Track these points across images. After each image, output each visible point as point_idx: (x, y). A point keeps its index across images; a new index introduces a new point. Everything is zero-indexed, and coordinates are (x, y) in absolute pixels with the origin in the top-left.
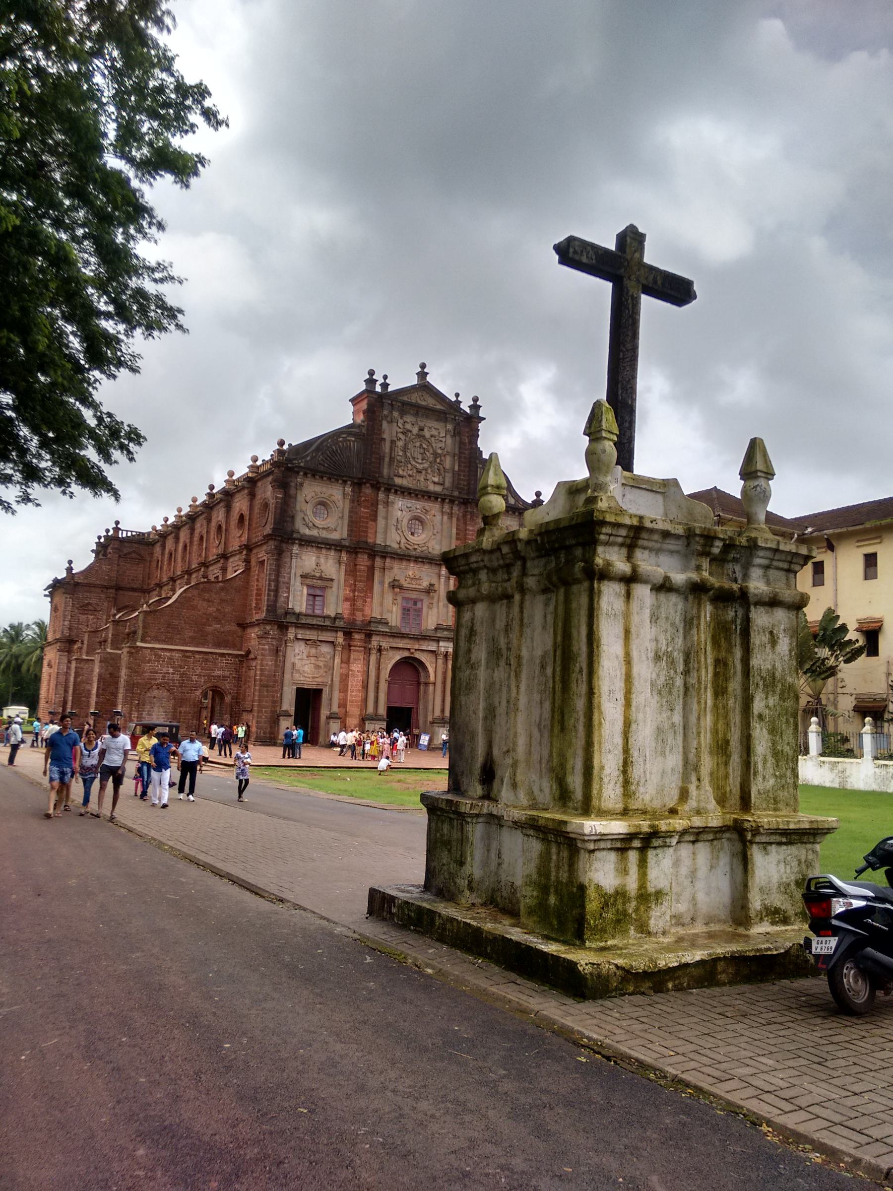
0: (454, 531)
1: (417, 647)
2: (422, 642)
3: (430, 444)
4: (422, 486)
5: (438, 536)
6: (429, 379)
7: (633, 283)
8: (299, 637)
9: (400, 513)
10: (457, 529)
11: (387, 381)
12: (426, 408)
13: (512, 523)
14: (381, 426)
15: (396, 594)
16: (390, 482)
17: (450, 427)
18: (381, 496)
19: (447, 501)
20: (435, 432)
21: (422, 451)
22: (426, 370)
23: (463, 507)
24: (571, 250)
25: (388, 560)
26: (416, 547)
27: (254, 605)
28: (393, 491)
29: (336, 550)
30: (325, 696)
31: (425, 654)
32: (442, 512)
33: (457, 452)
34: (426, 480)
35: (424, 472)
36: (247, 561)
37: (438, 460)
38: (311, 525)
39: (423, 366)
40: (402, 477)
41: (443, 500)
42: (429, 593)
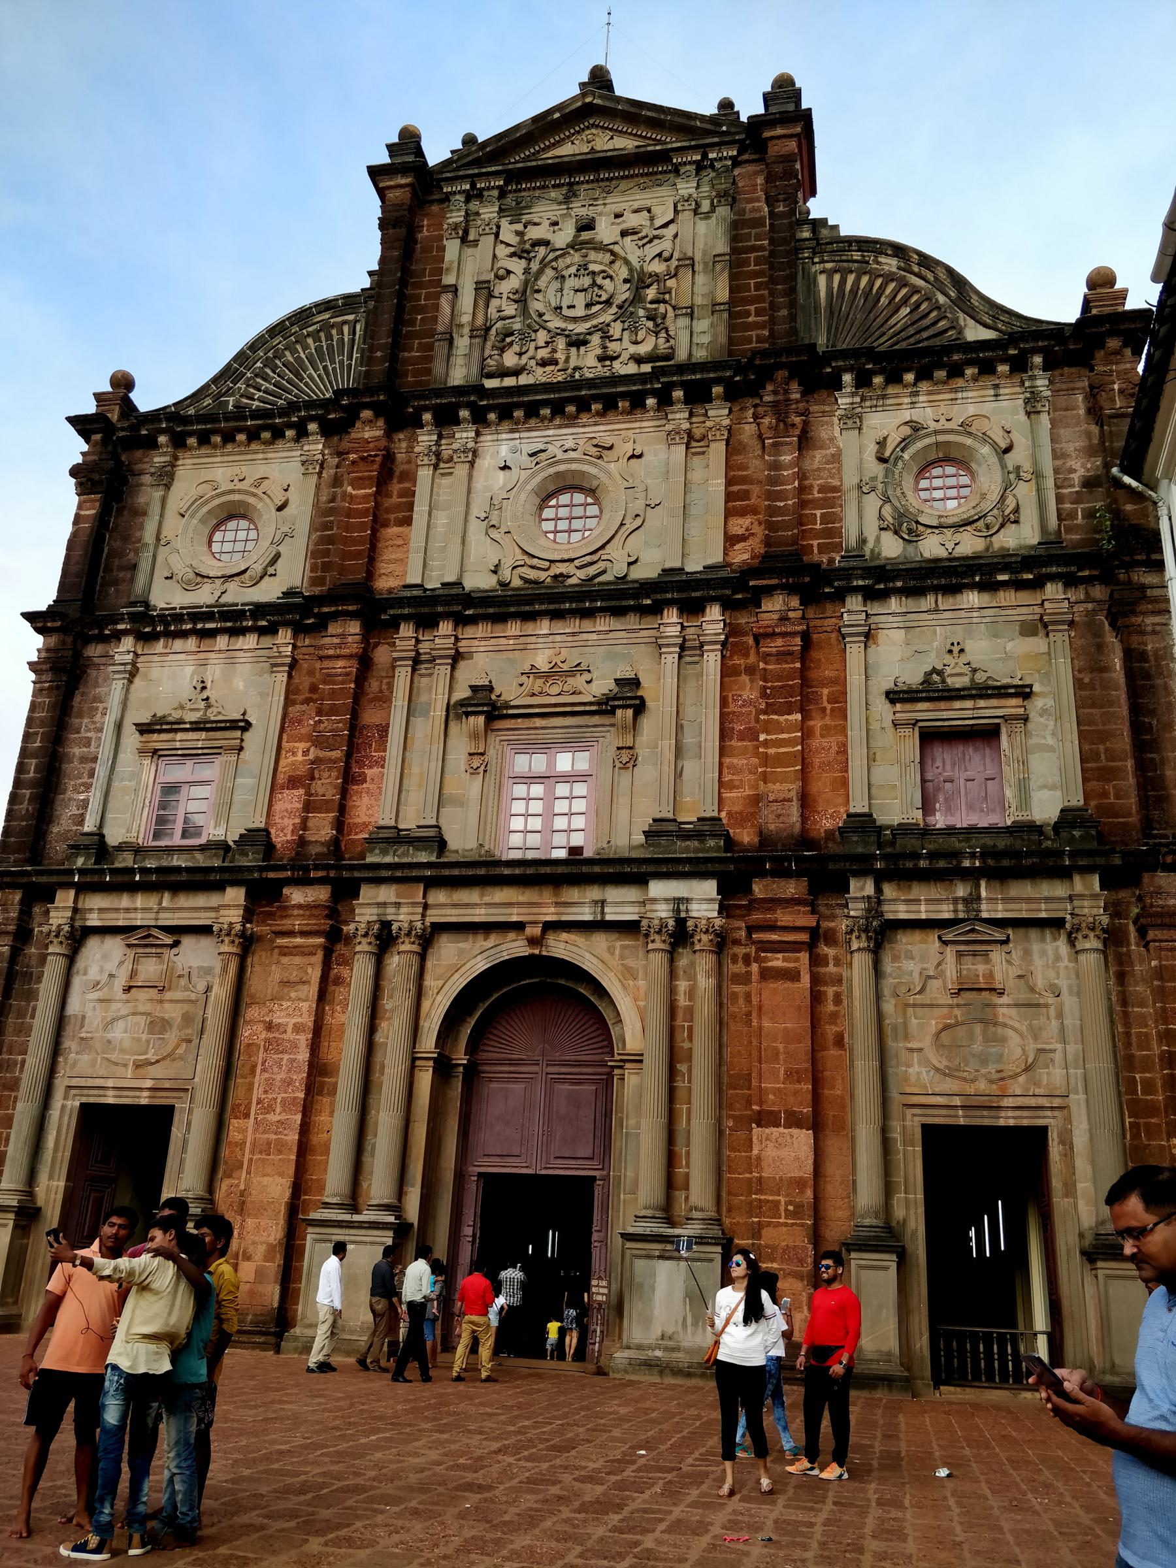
1: (550, 914)
2: (572, 894)
8: (93, 920)
10: (729, 482)
13: (988, 408)
15: (474, 736)
20: (632, 220)
21: (587, 281)
28: (464, 413)
29: (262, 632)
30: (176, 1132)
31: (601, 941)
35: (596, 339)
37: (651, 293)
40: (516, 372)
41: (665, 401)
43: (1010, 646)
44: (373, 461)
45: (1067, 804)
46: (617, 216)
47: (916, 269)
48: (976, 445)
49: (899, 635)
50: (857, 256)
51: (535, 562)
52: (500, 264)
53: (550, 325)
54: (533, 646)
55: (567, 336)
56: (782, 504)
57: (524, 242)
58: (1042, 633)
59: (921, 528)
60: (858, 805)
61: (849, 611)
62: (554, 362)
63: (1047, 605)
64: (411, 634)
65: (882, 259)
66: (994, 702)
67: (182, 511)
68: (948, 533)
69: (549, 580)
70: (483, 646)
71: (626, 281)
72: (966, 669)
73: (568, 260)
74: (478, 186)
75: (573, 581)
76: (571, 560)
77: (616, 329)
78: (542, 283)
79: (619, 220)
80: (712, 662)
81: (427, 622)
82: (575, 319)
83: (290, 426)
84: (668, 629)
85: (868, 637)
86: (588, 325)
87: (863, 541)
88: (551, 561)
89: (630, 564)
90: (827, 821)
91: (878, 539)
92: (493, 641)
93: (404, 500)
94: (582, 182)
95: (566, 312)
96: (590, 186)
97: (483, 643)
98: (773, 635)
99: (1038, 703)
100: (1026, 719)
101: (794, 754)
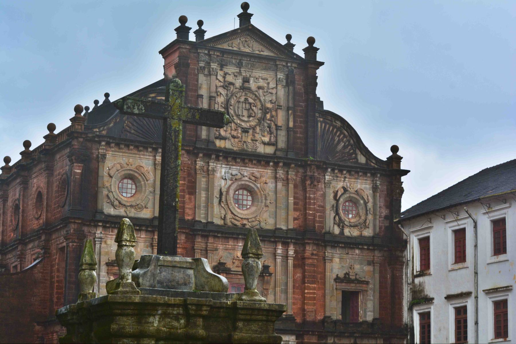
0: (291, 200)
3: (257, 97)
4: (250, 148)
5: (272, 209)
6: (254, 21)
7: (176, 121)
9: (223, 182)
10: (294, 198)
11: (203, 28)
12: (251, 56)
14: (197, 81)
16: (211, 147)
17: (281, 76)
18: (200, 163)
19: (281, 164)
20: (262, 83)
21: (248, 106)
22: (249, 11)
23: (301, 170)
24: (125, 107)
25: (211, 240)
26: (245, 222)
27: (55, 300)
28: (213, 156)
29: (147, 231)
32: (276, 178)
33: (291, 105)
34: (254, 140)
35: (251, 131)
36: (46, 249)
37: (268, 116)
38: (116, 203)
39: (245, 6)
41: (276, 165)
42: (263, 276)
43: (364, 268)
44: (185, 172)
45: (375, 317)
46: (257, 79)
47: (346, 128)
48: (360, 199)
49: (337, 260)
50: (329, 118)
51: (237, 218)
52: (218, 91)
53: (235, 121)
54: (236, 249)
55: (242, 128)
56: (311, 212)
57: (225, 81)
58: (372, 264)
59: (345, 226)
60: (328, 314)
61: (327, 252)
62: (238, 138)
63: (375, 257)
64: (200, 240)
65: (337, 122)
66: (360, 285)
67: (112, 175)
68: (352, 228)
69: (240, 225)
70: (221, 247)
71: (260, 109)
72: (354, 274)
73: (241, 94)
74: (211, 53)
75: (247, 227)
76: (248, 219)
77: (258, 129)
78: (233, 102)
79: (256, 81)
80: (291, 263)
81: (206, 237)
82: (243, 121)
83: (150, 147)
84: (279, 250)
85: (331, 260)
86: (248, 124)
87: (330, 228)
88: (242, 218)
89: (265, 223)
90: (320, 317)
91: (334, 226)
92: (224, 246)
93: (190, 184)
94: (244, 60)
95: (241, 117)
96: (248, 62)
97: (221, 246)
98: (310, 258)
99: (370, 286)
100: (367, 291)
101: (314, 298)
